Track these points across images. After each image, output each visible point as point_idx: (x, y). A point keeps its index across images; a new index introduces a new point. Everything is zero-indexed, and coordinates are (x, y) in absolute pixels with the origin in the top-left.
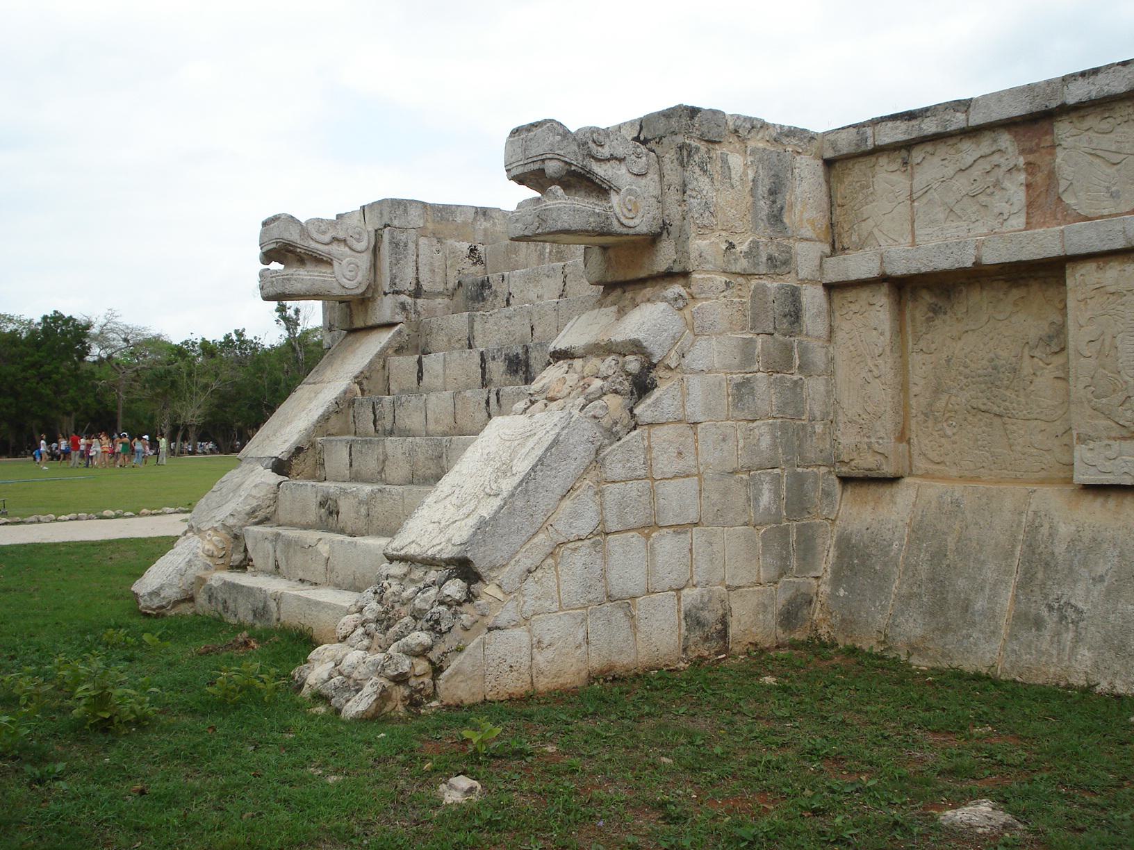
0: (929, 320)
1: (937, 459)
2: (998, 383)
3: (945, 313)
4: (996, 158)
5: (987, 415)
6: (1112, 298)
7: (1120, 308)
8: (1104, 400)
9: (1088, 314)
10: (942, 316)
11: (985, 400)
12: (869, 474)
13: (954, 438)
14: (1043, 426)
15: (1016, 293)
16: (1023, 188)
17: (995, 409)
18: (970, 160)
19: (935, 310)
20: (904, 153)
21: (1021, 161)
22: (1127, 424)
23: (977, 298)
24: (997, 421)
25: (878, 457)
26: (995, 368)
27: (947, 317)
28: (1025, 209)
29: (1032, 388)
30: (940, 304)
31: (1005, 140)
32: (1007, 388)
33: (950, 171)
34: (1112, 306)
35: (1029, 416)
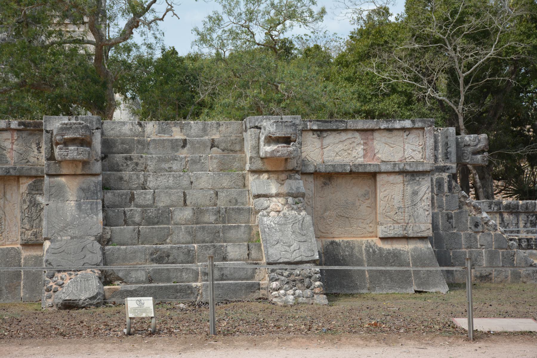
0: (322, 187)
4: (353, 140)
9: (384, 189)
10: (327, 186)
14: (363, 221)
15: (354, 181)
17: (346, 215)
18: (344, 138)
19: (325, 184)
20: (319, 133)
21: (362, 142)
23: (340, 181)
24: (347, 220)
26: (347, 203)
31: (357, 135)
33: (337, 140)
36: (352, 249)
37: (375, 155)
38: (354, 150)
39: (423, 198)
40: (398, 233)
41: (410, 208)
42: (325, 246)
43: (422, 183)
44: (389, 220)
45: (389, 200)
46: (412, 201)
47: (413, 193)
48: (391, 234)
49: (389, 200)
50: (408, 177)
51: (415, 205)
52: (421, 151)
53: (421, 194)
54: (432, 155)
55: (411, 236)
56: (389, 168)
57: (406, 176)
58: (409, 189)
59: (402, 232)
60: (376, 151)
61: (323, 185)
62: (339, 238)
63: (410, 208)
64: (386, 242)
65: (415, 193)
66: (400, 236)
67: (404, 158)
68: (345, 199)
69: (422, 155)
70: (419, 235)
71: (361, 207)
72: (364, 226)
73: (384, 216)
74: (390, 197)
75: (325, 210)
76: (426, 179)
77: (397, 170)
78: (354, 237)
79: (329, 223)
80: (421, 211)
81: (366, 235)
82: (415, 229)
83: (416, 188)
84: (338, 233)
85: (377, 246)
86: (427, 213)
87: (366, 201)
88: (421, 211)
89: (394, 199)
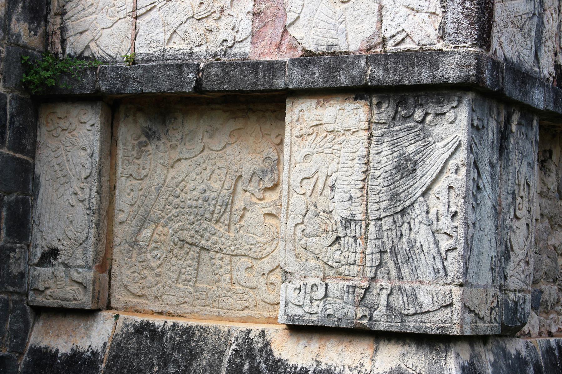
0: (142, 145)
1: (138, 291)
2: (207, 215)
3: (159, 139)
5: (194, 248)
6: (330, 136)
7: (336, 146)
8: (314, 239)
9: (305, 151)
10: (155, 142)
11: (192, 233)
12: (64, 304)
13: (157, 271)
14: (249, 262)
16: (250, 16)
19: (150, 135)
22: (335, 265)
25: (76, 287)
26: (206, 200)
27: (160, 143)
28: (249, 39)
29: (242, 223)
30: (154, 129)
32: (217, 221)
34: (328, 145)
35: (236, 252)
36: (193, 355)
37: (285, 31)
38: (225, 20)
39: (436, 188)
40: (339, 315)
41: (387, 223)
42: (119, 338)
43: (436, 131)
44: (313, 262)
45: (319, 189)
46: (395, 197)
47: (398, 168)
48: (315, 313)
49: (319, 189)
50: (387, 110)
51: (403, 212)
52: (439, 11)
53: (428, 170)
54: (466, 23)
55: (381, 326)
56: (317, 77)
57: (379, 105)
58: (385, 158)
59: (350, 310)
60: (291, 17)
61: (143, 139)
62: (170, 315)
63: (387, 223)
64: (303, 342)
65: (406, 168)
66: (344, 325)
67: (378, 40)
68: (203, 186)
69: (442, 27)
70: (412, 326)
71: (248, 215)
72: (254, 282)
73: (300, 250)
74: (321, 182)
75: (144, 222)
76: (450, 116)
77: (344, 80)
78: (220, 317)
79: (154, 265)
80: (422, 236)
81: (256, 313)
82: (398, 301)
83: (411, 149)
84: (174, 301)
85: (270, 353)
86: (445, 244)
87: (268, 194)
88: (422, 236)
89: (333, 187)
